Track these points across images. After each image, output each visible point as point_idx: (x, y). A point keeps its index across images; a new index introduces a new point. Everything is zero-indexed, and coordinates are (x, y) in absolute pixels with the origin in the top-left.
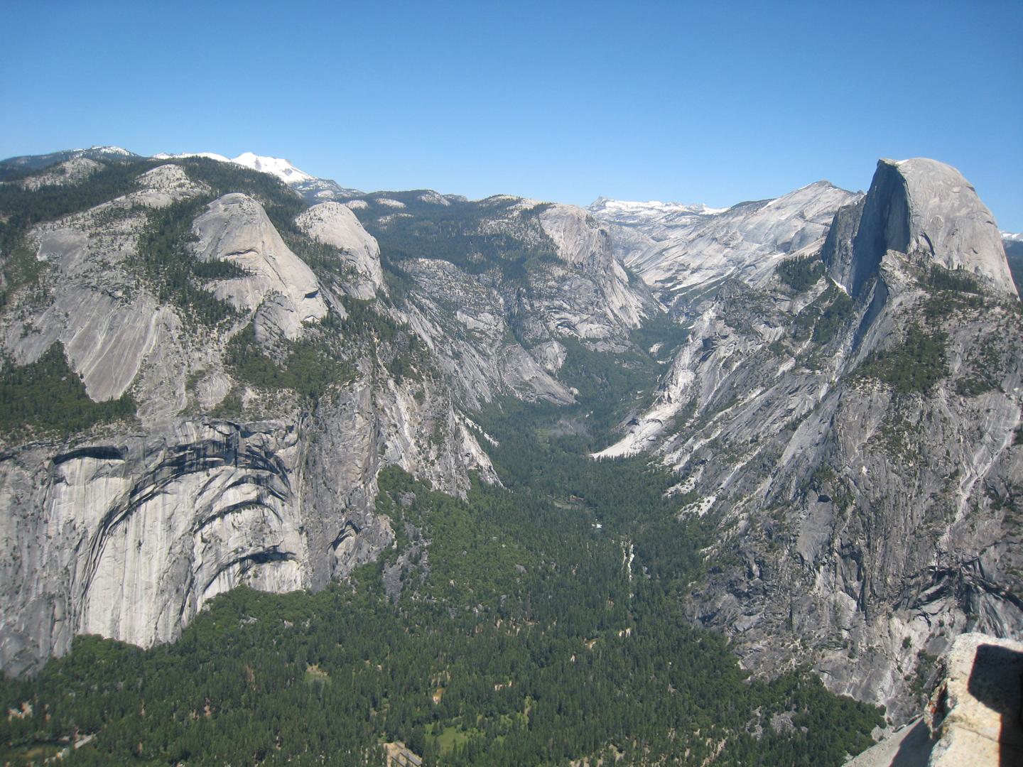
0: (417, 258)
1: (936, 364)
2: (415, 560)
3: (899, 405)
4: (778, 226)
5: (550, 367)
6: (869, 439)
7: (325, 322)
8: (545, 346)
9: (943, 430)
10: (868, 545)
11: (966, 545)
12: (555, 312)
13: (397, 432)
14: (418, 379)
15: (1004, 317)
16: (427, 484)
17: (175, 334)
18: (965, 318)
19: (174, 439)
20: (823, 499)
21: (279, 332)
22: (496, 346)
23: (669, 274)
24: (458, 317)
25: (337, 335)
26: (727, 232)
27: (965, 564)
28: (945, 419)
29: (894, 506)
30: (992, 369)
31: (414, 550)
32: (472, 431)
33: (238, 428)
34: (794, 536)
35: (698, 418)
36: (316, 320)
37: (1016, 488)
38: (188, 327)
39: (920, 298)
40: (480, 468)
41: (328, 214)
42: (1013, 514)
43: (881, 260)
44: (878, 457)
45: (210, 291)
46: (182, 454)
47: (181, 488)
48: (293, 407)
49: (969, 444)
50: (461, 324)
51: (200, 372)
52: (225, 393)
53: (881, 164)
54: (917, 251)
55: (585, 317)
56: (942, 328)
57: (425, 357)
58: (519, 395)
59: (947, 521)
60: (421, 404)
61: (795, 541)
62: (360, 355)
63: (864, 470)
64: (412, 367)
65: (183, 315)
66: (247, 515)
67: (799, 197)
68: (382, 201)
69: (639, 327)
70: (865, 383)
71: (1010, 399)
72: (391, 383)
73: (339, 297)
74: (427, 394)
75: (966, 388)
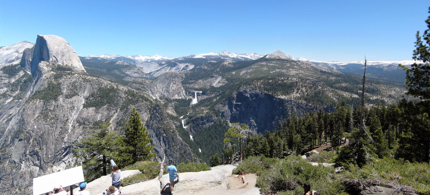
1: (58, 91)
3: (46, 105)
4: (8, 55)
10: (40, 149)
11: (72, 138)
20: (20, 140)
27: (73, 143)
28: (62, 106)
29: (48, 134)
30: (75, 90)
34: (10, 155)
37: (85, 119)
39: (52, 74)
42: (85, 126)
43: (39, 64)
44: (40, 122)
49: (70, 111)
53: (38, 36)
54: (52, 61)
56: (59, 81)
59: (66, 133)
61: (11, 157)
67: (15, 46)
70: (33, 101)
75: (68, 97)
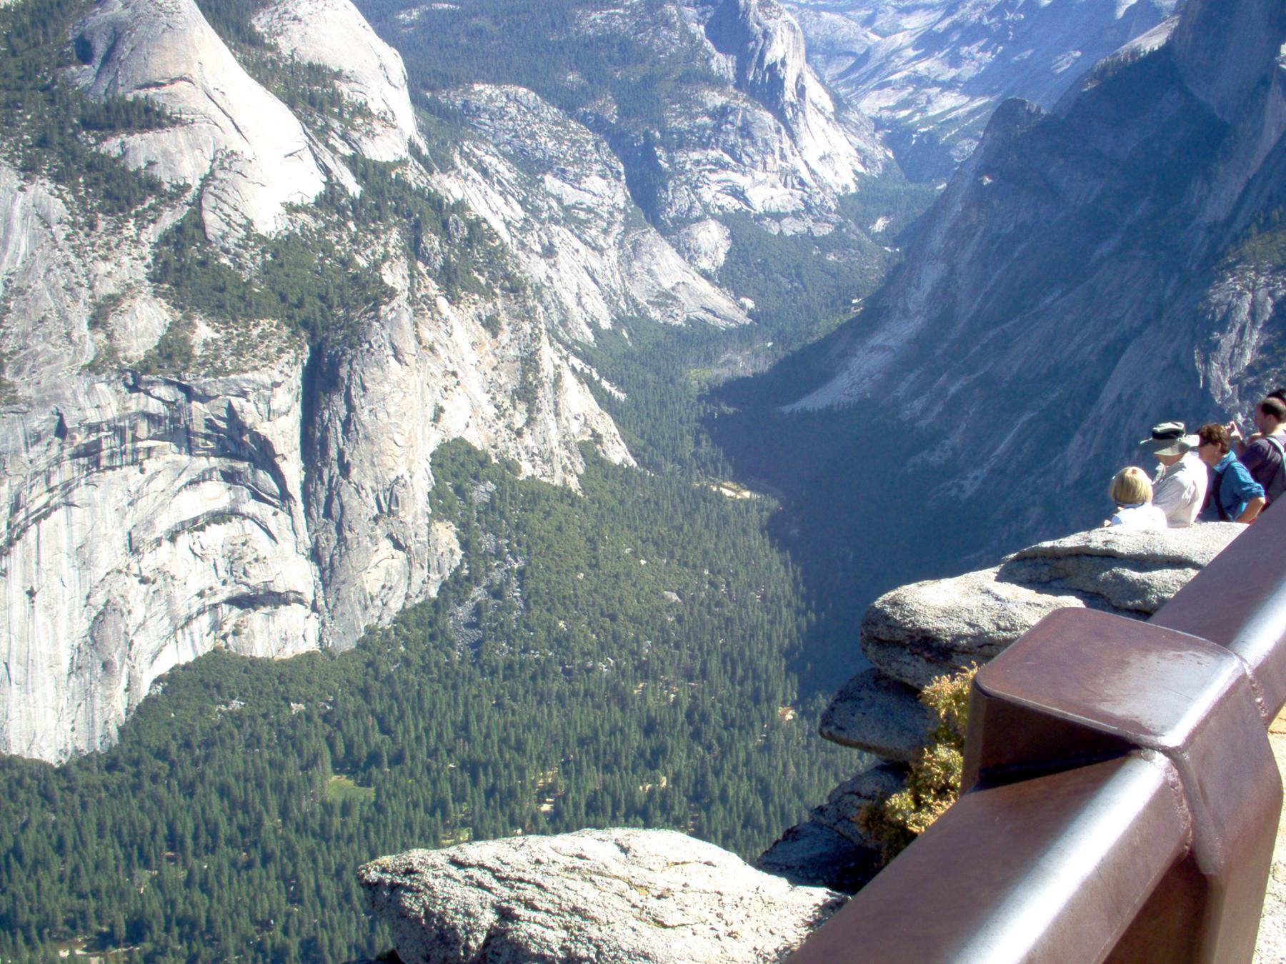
0: (471, 83)
2: (496, 593)
5: (705, 264)
12: (710, 171)
13: (458, 384)
14: (487, 293)
16: (512, 467)
17: (61, 232)
19: (75, 412)
21: (244, 222)
22: (614, 234)
23: (904, 94)
25: (345, 224)
31: (497, 576)
32: (583, 378)
33: (187, 390)
38: (82, 220)
40: (597, 438)
41: (310, 9)
45: (114, 155)
46: (93, 437)
47: (97, 495)
48: (281, 351)
51: (110, 297)
52: (161, 332)
55: (760, 175)
57: (496, 257)
58: (655, 314)
60: (495, 335)
62: (386, 257)
65: (69, 198)
66: (216, 535)
72: (442, 303)
73: (344, 159)
74: (504, 318)
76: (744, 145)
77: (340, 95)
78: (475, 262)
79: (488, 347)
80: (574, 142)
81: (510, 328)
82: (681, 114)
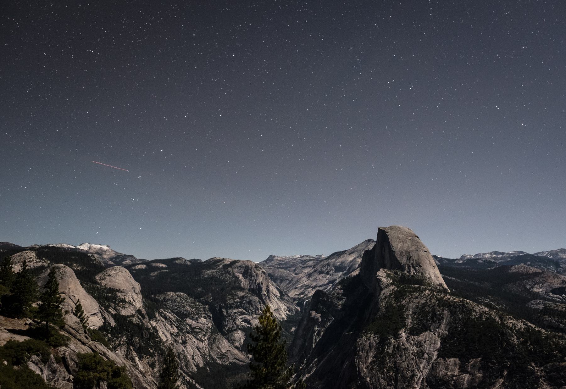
5: (237, 344)
6: (370, 363)
7: (101, 328)
8: (234, 333)
9: (405, 354)
12: (239, 315)
14: (152, 355)
15: (429, 295)
18: (412, 297)
22: (208, 335)
23: (301, 291)
24: (187, 321)
25: (107, 335)
26: (328, 268)
28: (405, 348)
35: (306, 364)
36: (96, 328)
39: (393, 290)
50: (188, 325)
53: (379, 229)
55: (255, 316)
56: (402, 303)
58: (219, 361)
60: (153, 369)
62: (120, 345)
63: (368, 379)
64: (150, 349)
68: (154, 264)
69: (285, 319)
71: (435, 335)
74: (157, 363)
75: (413, 332)
76: (249, 307)
77: (117, 296)
78: (150, 346)
79: (149, 373)
80: (196, 308)
81: (158, 366)
82: (231, 299)
